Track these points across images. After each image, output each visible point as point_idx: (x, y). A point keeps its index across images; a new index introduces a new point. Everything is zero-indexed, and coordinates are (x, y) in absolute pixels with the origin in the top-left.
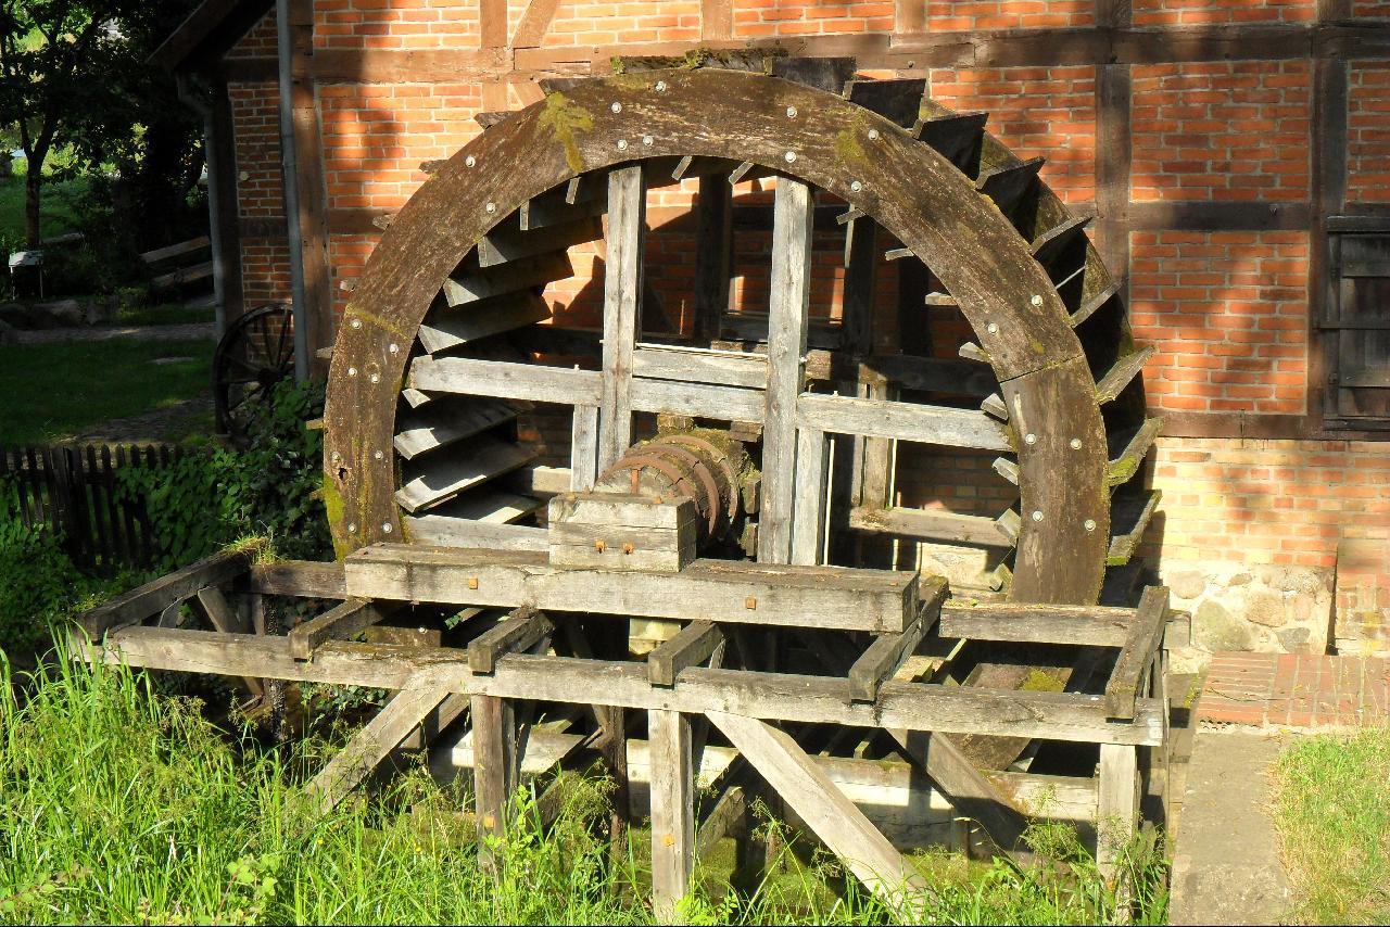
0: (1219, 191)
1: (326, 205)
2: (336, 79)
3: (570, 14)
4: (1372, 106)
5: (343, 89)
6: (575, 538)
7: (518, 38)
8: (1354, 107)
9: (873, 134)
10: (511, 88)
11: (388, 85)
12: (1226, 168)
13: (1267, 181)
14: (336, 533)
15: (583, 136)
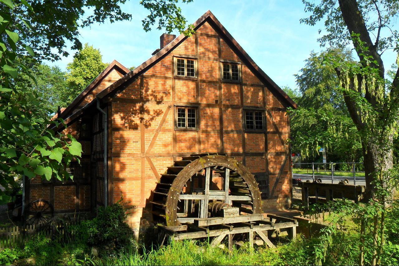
1: (113, 177)
2: (116, 157)
5: (117, 158)
6: (227, 214)
7: (147, 151)
9: (238, 163)
14: (167, 222)
15: (204, 163)
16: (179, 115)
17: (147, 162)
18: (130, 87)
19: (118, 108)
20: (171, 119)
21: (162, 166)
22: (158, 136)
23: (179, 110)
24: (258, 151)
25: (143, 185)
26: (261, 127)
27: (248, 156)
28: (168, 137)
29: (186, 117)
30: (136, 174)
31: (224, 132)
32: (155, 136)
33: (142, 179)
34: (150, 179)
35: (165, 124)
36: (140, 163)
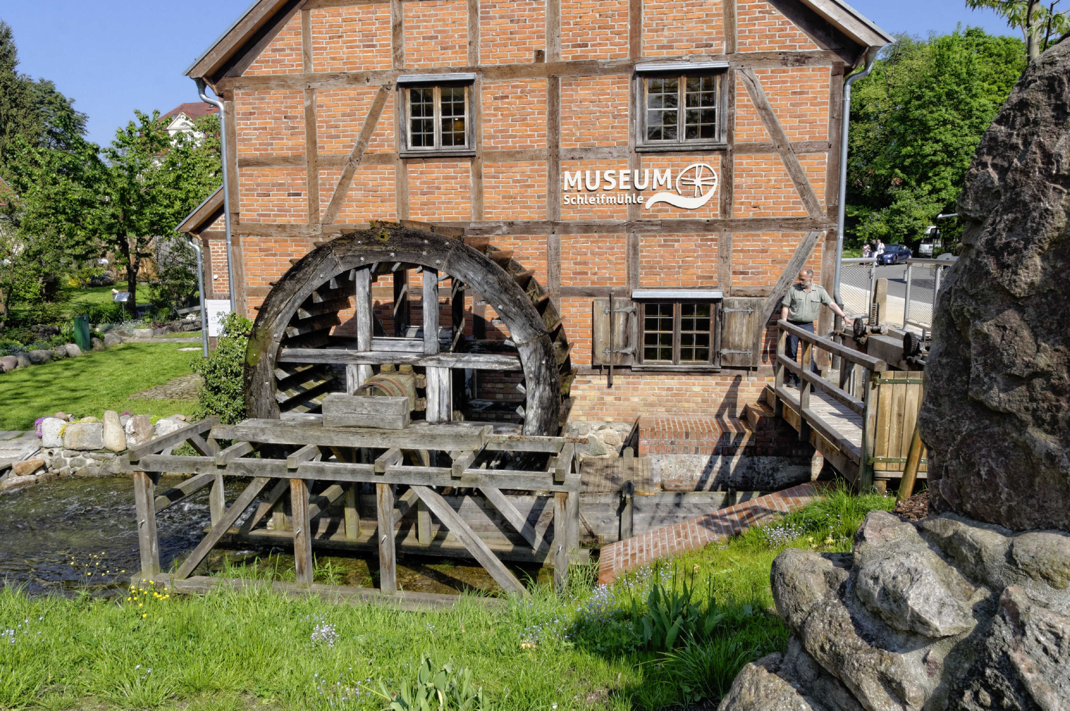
0: (593, 283)
1: (245, 285)
4: (648, 251)
7: (324, 220)
8: (642, 251)
12: (595, 274)
13: (611, 279)
16: (416, 111)
20: (391, 124)
22: (355, 176)
23: (415, 98)
24: (688, 216)
26: (708, 132)
27: (652, 230)
28: (382, 179)
29: (438, 118)
32: (346, 178)
35: (375, 140)
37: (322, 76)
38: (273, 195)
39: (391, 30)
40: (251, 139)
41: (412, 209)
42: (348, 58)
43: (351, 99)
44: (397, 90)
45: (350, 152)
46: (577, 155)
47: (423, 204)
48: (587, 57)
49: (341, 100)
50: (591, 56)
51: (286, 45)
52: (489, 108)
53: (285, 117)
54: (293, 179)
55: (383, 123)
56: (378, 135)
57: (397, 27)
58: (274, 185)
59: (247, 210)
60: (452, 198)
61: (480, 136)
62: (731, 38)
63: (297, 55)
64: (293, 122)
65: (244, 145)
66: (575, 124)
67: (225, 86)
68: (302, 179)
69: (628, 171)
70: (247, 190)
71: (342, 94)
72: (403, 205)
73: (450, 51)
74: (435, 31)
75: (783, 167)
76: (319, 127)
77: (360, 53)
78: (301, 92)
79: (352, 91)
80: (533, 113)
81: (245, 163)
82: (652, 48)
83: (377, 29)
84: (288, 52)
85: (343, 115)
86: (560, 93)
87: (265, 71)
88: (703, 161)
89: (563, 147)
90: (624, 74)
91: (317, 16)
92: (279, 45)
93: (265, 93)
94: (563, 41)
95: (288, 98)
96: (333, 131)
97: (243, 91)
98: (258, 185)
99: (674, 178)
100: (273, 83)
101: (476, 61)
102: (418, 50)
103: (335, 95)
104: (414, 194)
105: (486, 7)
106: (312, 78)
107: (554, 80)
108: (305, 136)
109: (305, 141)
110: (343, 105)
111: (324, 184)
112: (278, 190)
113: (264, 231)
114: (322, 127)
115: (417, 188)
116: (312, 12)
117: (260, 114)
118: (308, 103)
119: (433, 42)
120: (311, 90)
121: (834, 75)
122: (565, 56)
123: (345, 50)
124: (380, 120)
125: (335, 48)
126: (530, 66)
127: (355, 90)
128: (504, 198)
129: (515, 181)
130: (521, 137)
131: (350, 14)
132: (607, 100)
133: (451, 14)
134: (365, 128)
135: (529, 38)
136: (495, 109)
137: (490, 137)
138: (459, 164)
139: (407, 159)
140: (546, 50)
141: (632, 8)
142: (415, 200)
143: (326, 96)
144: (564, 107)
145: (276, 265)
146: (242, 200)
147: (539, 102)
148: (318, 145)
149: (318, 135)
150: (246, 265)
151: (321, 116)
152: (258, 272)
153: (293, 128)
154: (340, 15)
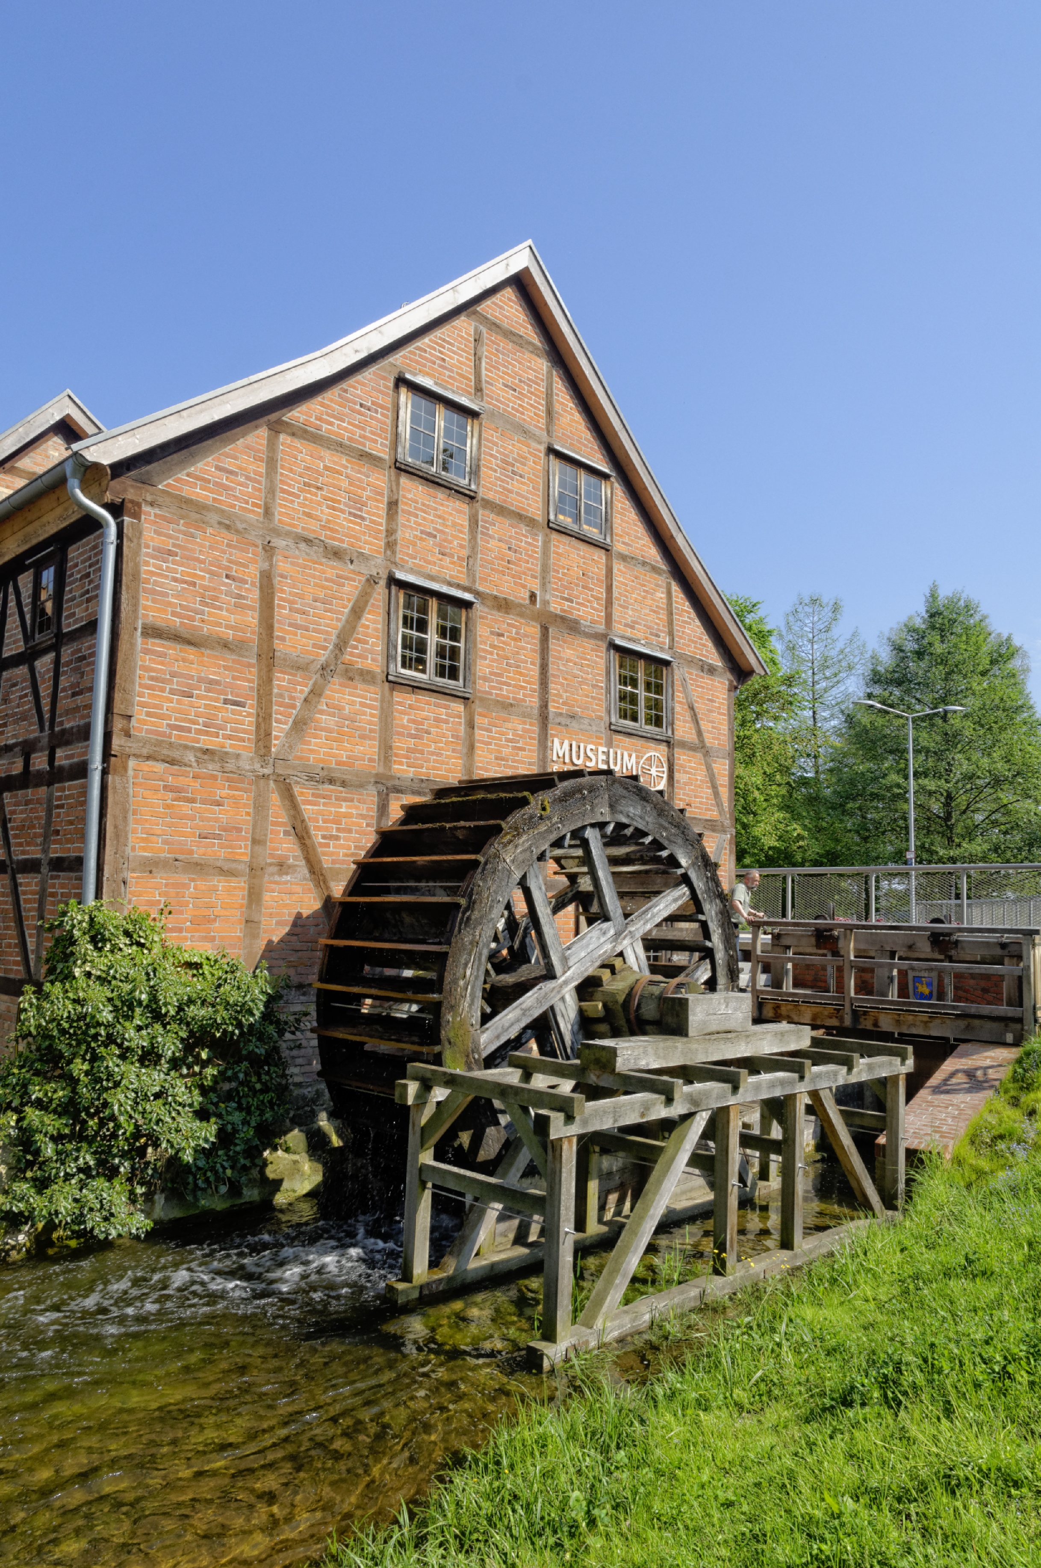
1: (128, 850)
3: (309, 743)
7: (278, 753)
10: (272, 784)
11: (188, 769)
17: (275, 799)
18: (228, 456)
19: (169, 536)
20: (376, 630)
21: (334, 822)
25: (254, 896)
30: (231, 847)
31: (551, 716)
32: (316, 693)
33: (255, 870)
34: (287, 874)
35: (356, 648)
36: (246, 798)
37: (288, 534)
38: (199, 697)
39: (384, 506)
40: (166, 595)
41: (396, 755)
42: (328, 521)
43: (327, 580)
44: (389, 586)
45: (324, 656)
46: (563, 720)
47: (409, 750)
48: (572, 614)
49: (314, 577)
50: (575, 614)
51: (241, 468)
52: (485, 644)
53: (227, 577)
54: (234, 678)
55: (367, 627)
56: (359, 640)
57: (393, 505)
58: (200, 680)
59: (148, 714)
60: (441, 749)
61: (475, 674)
62: (671, 634)
63: (254, 488)
64: (240, 588)
65: (154, 601)
66: (562, 685)
67: (125, 490)
68: (249, 681)
69: (605, 750)
70: (152, 678)
71: (315, 569)
72: (386, 750)
73: (448, 560)
74: (435, 529)
75: (704, 767)
76: (280, 606)
77: (343, 521)
78: (257, 546)
79: (332, 569)
80: (526, 662)
81: (153, 632)
82: (620, 622)
83: (369, 498)
84: (242, 480)
85: (315, 600)
86: (551, 646)
87: (198, 493)
88: (656, 750)
89: (551, 709)
90: (600, 643)
91: (289, 446)
92: (229, 462)
93: (197, 528)
94: (554, 590)
95: (235, 547)
96: (299, 618)
97: (158, 511)
98: (173, 675)
99: (638, 763)
100: (213, 518)
101: (474, 581)
102: (415, 544)
103: (305, 567)
104: (399, 734)
105: (486, 522)
106: (277, 532)
107: (545, 630)
108: (257, 615)
109: (256, 621)
110: (316, 585)
111: (281, 696)
112: (208, 690)
113: (176, 754)
114: (284, 608)
115: (403, 726)
116: (282, 437)
117: (188, 558)
118: (266, 566)
119: (431, 541)
120: (269, 549)
121: (729, 691)
122: (555, 607)
123: (324, 508)
124: (363, 621)
125: (311, 501)
126: (521, 605)
127: (333, 568)
128: (497, 758)
129: (508, 740)
130: (515, 686)
131: (335, 463)
132: (588, 666)
133: (451, 514)
134: (344, 627)
135: (525, 574)
136: (492, 646)
137: (485, 679)
138: (452, 704)
139: (395, 684)
140: (538, 593)
141: (607, 577)
142: (400, 744)
143: (292, 563)
144: (553, 663)
145: (193, 818)
146: (141, 695)
147: (533, 650)
148: (276, 633)
149: (276, 617)
150: (135, 813)
151: (284, 591)
152: (158, 829)
153: (239, 597)
154: (321, 458)
